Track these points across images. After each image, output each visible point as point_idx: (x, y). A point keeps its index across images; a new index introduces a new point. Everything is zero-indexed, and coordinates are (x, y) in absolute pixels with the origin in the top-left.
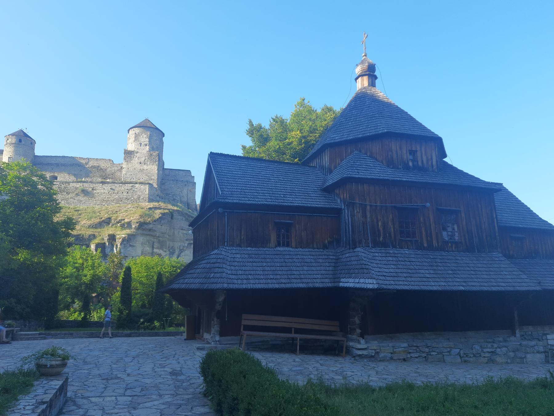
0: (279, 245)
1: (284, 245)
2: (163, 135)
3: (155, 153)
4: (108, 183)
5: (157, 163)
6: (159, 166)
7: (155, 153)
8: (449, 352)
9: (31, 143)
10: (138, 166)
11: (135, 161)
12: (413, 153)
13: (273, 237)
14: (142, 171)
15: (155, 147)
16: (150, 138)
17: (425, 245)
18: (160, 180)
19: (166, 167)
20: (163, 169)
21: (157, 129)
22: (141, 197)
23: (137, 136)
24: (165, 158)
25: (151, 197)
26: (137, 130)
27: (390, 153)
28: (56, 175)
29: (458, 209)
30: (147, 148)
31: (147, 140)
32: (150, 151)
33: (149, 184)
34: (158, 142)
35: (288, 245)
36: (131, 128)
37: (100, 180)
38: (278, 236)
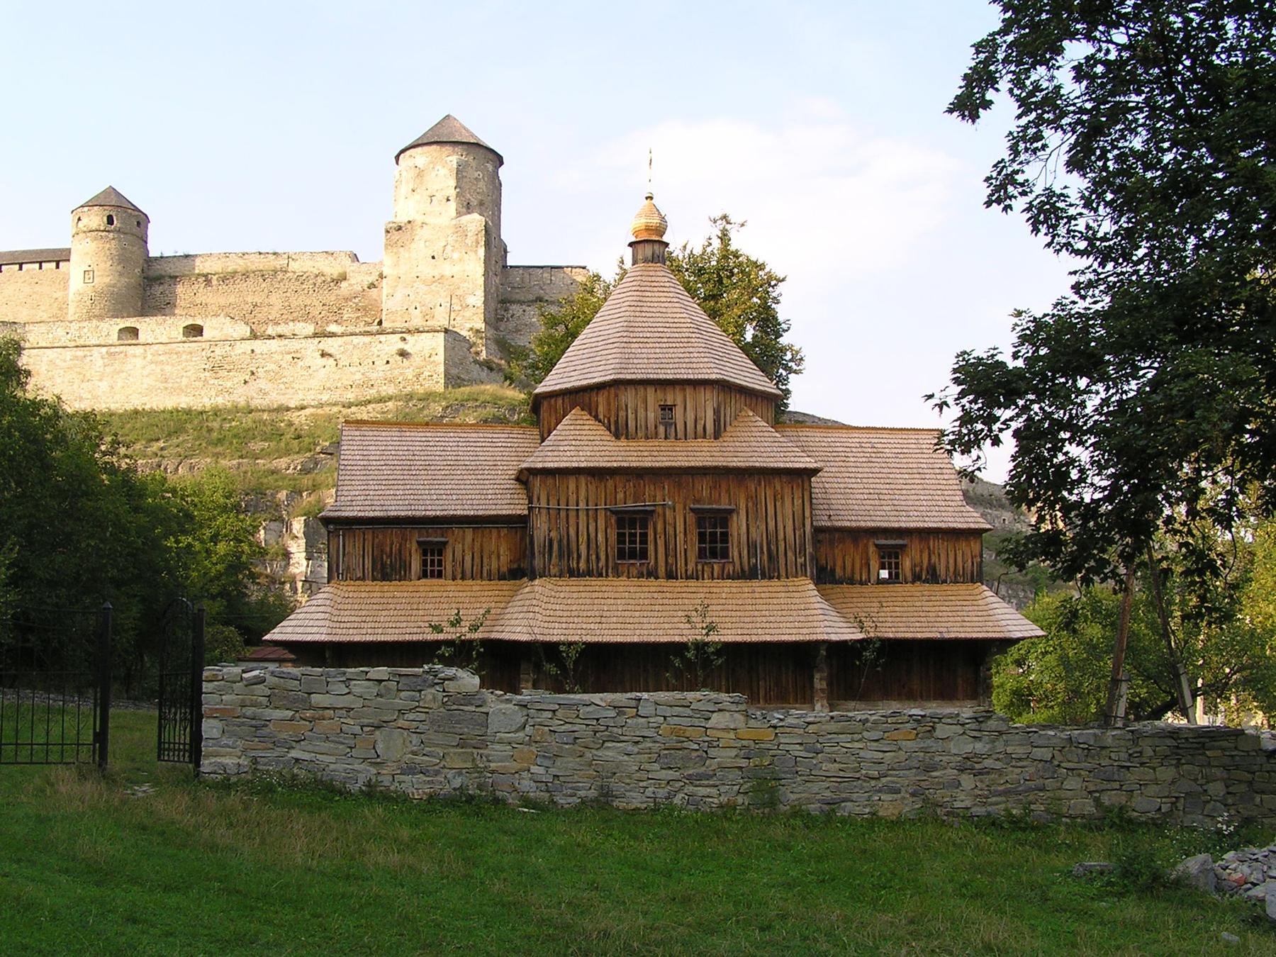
0: (425, 575)
1: (432, 576)
2: (499, 160)
3: (475, 221)
4: (333, 335)
5: (481, 251)
7: (475, 221)
9: (139, 223)
10: (428, 270)
11: (419, 248)
12: (667, 408)
13: (416, 566)
15: (474, 203)
16: (460, 172)
17: (662, 570)
18: (493, 305)
19: (511, 261)
20: (505, 267)
21: (478, 145)
22: (427, 374)
23: (420, 173)
24: (507, 234)
25: (454, 371)
26: (421, 157)
27: (622, 414)
28: (199, 322)
29: (733, 507)
30: (453, 206)
31: (453, 183)
32: (459, 214)
33: (446, 331)
34: (481, 184)
35: (440, 575)
36: (403, 151)
37: (310, 329)
38: (424, 563)
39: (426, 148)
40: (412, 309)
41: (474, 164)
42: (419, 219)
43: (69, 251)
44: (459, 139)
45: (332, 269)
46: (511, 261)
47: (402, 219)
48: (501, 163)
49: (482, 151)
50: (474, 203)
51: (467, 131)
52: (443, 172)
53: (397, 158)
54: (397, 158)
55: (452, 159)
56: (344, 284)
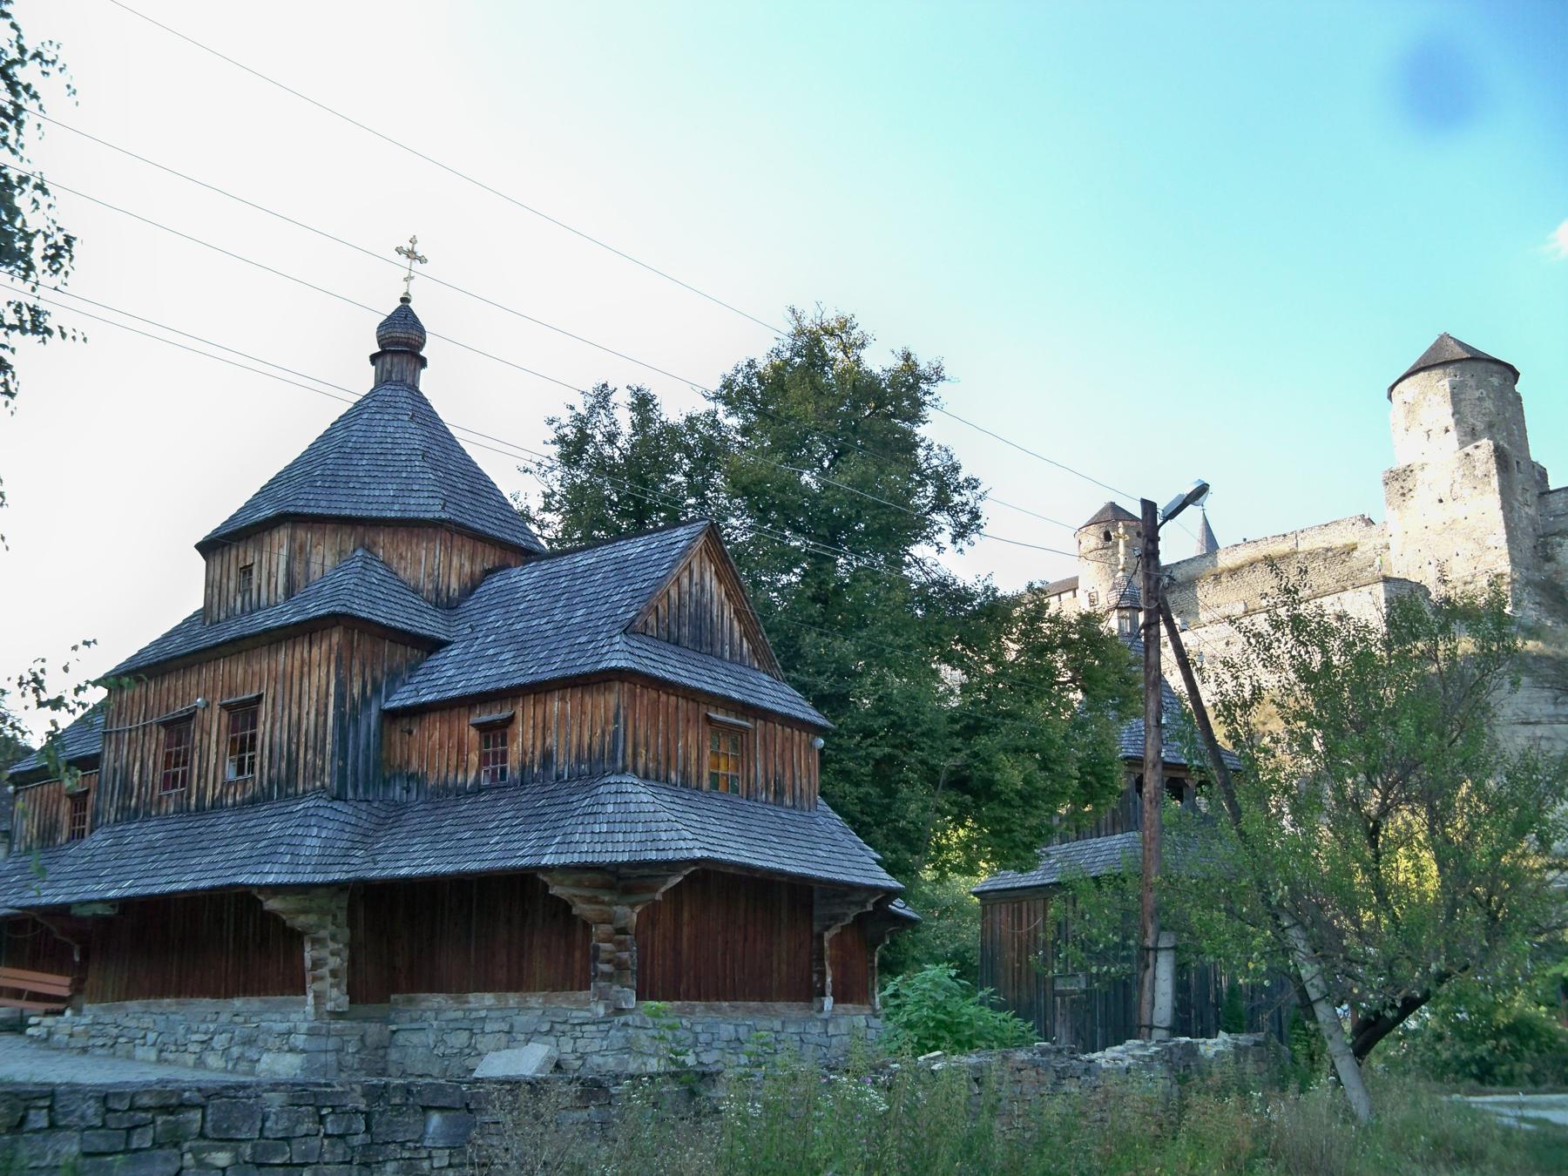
6: (1506, 492)
8: (144, 1037)
11: (1423, 496)
14: (1449, 526)
15: (1480, 426)
18: (1528, 543)
19: (1553, 484)
23: (1410, 407)
30: (1453, 434)
32: (1463, 444)
34: (1488, 404)
39: (1412, 378)
40: (1425, 566)
41: (1472, 382)
42: (1416, 462)
43: (1076, 579)
44: (1448, 357)
45: (1338, 539)
46: (1553, 484)
47: (1400, 464)
48: (1516, 374)
49: (1480, 366)
50: (1480, 426)
51: (1461, 344)
52: (1439, 398)
53: (1390, 397)
54: (1390, 397)
55: (1438, 385)
56: (1355, 554)
